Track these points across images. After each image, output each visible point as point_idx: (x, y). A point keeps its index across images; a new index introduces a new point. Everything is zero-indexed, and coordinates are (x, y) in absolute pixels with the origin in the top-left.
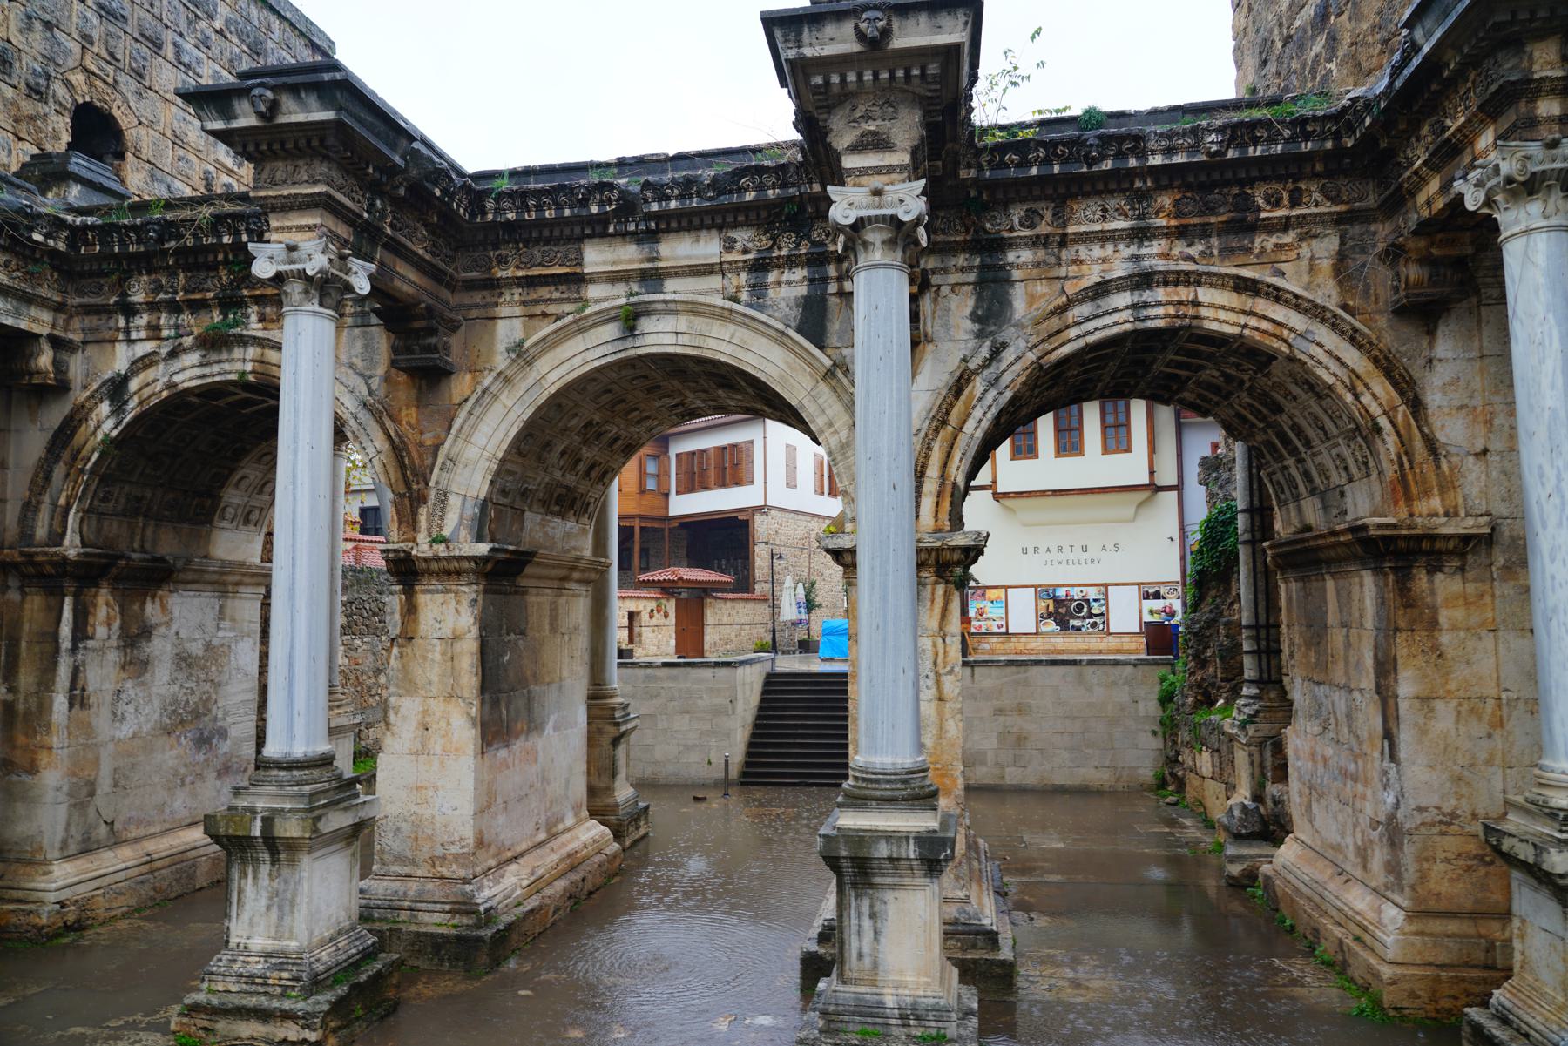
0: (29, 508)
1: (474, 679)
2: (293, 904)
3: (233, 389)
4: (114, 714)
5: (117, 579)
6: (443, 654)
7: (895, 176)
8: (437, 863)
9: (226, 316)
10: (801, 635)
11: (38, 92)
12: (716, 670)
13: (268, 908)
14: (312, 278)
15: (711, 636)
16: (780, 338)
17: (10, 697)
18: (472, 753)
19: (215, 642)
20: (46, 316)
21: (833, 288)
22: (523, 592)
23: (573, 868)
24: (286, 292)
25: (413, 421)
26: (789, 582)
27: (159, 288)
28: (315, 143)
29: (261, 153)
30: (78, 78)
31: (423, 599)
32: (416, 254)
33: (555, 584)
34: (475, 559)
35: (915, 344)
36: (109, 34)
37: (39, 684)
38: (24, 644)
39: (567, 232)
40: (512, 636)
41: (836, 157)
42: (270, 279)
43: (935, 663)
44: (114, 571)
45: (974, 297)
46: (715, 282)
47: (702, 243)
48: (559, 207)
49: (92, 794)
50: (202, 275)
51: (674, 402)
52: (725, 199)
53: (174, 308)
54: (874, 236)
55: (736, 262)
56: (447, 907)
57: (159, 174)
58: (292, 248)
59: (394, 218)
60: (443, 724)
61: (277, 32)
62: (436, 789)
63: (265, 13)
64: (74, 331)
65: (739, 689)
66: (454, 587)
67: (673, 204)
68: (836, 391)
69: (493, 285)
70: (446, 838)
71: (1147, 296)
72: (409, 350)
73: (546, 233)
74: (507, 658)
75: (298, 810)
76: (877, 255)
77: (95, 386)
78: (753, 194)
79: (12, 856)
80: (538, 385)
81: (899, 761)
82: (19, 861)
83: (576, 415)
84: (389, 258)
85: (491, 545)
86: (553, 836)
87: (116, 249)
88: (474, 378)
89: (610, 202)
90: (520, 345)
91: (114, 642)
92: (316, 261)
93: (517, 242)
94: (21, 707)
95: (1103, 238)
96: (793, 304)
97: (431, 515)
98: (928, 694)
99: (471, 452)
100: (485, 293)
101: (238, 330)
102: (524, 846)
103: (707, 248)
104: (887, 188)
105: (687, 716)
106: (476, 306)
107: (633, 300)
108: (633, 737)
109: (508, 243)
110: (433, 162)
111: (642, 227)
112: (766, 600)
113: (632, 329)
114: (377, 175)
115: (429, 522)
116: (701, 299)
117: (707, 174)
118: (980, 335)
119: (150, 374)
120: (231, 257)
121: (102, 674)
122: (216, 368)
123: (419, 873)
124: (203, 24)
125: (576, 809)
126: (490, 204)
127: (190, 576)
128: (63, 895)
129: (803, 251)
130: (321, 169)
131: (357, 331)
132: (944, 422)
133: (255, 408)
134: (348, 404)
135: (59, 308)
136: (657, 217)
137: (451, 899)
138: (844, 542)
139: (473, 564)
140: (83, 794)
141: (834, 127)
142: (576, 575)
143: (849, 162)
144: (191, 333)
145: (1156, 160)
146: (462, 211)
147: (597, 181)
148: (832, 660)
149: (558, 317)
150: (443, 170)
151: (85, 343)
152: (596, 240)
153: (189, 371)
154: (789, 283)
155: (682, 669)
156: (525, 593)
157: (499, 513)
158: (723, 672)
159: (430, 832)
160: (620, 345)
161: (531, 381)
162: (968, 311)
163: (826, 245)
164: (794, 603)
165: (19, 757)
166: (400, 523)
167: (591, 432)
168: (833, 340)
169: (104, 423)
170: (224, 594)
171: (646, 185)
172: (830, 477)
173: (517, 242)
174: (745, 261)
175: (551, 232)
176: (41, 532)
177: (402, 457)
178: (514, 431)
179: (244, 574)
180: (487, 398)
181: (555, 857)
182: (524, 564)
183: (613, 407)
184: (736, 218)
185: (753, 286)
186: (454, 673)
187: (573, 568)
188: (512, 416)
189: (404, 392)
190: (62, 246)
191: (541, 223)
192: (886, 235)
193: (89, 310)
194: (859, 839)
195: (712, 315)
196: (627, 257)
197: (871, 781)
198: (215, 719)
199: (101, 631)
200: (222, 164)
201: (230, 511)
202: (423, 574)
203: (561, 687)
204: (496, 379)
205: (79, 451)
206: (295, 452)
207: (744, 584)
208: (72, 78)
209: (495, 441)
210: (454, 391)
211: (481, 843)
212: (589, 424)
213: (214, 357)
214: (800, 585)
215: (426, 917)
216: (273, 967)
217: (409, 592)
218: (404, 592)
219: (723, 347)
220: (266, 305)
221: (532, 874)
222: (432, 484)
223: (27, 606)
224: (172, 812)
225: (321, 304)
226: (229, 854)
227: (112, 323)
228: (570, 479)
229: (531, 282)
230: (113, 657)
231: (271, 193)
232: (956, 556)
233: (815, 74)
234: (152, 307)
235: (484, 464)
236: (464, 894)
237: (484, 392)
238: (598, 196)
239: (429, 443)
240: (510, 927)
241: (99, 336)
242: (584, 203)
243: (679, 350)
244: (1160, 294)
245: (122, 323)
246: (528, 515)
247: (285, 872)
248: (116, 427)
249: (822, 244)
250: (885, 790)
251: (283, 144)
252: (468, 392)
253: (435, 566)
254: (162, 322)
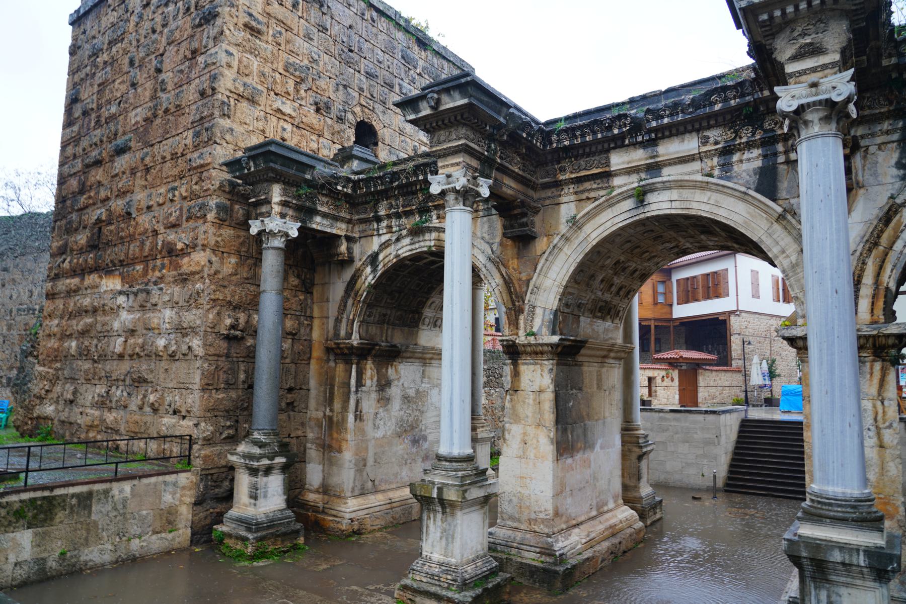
0: (338, 320)
1: (552, 416)
2: (453, 538)
3: (426, 256)
4: (375, 425)
5: (375, 356)
6: (534, 400)
7: (826, 72)
8: (532, 523)
9: (421, 218)
10: (766, 394)
11: (341, 119)
12: (706, 416)
13: (441, 538)
14: (459, 191)
15: (702, 394)
16: (743, 197)
17: (331, 414)
18: (551, 459)
19: (421, 389)
20: (344, 226)
21: (781, 159)
22: (580, 365)
23: (613, 535)
24: (446, 201)
25: (516, 267)
26: (756, 359)
27: (391, 207)
28: (459, 118)
29: (433, 128)
30: (358, 110)
31: (523, 368)
32: (514, 172)
33: (600, 360)
34: (551, 345)
35: (849, 190)
36: (371, 86)
37: (342, 408)
38: (336, 388)
39: (600, 147)
40: (574, 391)
41: (782, 66)
42: (439, 194)
43: (876, 420)
44: (374, 352)
45: (898, 151)
46: (696, 165)
47: (686, 142)
48: (594, 133)
49: (365, 465)
50: (410, 197)
51: (672, 245)
52: (701, 112)
53: (398, 216)
54: (813, 116)
55: (710, 151)
56: (538, 550)
57: (393, 150)
58: (449, 176)
59: (502, 153)
60: (534, 441)
61: (446, 69)
62: (531, 479)
63: (441, 60)
64: (355, 233)
65: (722, 428)
66: (540, 361)
67: (666, 121)
68: (786, 229)
69: (558, 185)
70: (537, 509)
72: (512, 227)
73: (587, 150)
74: (571, 404)
75: (455, 485)
76: (816, 129)
77: (364, 259)
78: (720, 105)
79: (332, 493)
80: (585, 241)
81: (849, 491)
82: (334, 495)
83: (609, 257)
84: (500, 176)
85: (560, 337)
86: (601, 514)
87: (372, 189)
88: (548, 240)
89: (625, 125)
90: (574, 218)
91: (374, 388)
92: (461, 181)
93: (571, 158)
94: (335, 419)
96: (752, 173)
97: (526, 320)
98: (870, 442)
99: (548, 283)
100: (553, 190)
101: (427, 224)
102: (583, 518)
103: (690, 145)
104: (821, 81)
105: (687, 445)
106: (549, 198)
107: (642, 183)
108: (651, 456)
109: (566, 159)
110: (521, 118)
111: (646, 138)
112: (740, 371)
113: (642, 201)
114: (492, 130)
115: (525, 324)
116: (687, 178)
117: (687, 98)
119: (388, 251)
120: (423, 186)
121: (369, 404)
122: (417, 245)
123: (522, 527)
124: (412, 72)
125: (615, 499)
126: (554, 138)
127: (408, 355)
128: (353, 515)
129: (758, 137)
130: (463, 131)
131: (485, 219)
132: (876, 244)
133: (437, 265)
134: (481, 260)
135: (349, 222)
136: (656, 130)
137: (540, 545)
138: (797, 332)
139: (550, 348)
140: (361, 465)
141: (778, 47)
142: (612, 355)
143: (790, 68)
144: (406, 228)
146: (538, 144)
147: (616, 114)
148: (789, 412)
149: (596, 199)
150: (527, 122)
151: (360, 238)
152: (617, 150)
153: (405, 248)
154: (749, 160)
155: (683, 414)
156: (581, 366)
157: (565, 318)
158: (711, 417)
159: (528, 504)
160: (635, 212)
161: (581, 238)
162: (893, 161)
163: (775, 131)
164: (760, 373)
165: (334, 444)
166: (510, 325)
167: (619, 267)
168: (783, 194)
169: (369, 277)
170: (425, 364)
171: (648, 111)
172: (783, 290)
173: (571, 158)
174: (716, 150)
175: (590, 149)
176: (343, 333)
177: (510, 287)
178: (572, 268)
179: (434, 354)
180: (556, 251)
181: (601, 527)
182: (580, 348)
183: (632, 251)
184: (708, 123)
185: (723, 165)
186: (540, 412)
187: (610, 351)
188: (571, 260)
189: (511, 252)
190: (350, 191)
191: (584, 144)
192: (822, 114)
193: (362, 221)
194: (816, 545)
195: (695, 187)
196: (638, 157)
197: (825, 504)
198: (421, 430)
199: (368, 382)
200: (422, 141)
201: (427, 320)
202: (522, 354)
203: (604, 423)
204: (560, 239)
205: (358, 292)
206: (452, 287)
207: (724, 360)
208: (355, 110)
209: (561, 276)
210: (537, 248)
211: (557, 514)
212: (618, 262)
213: (416, 239)
214: (764, 362)
215: (526, 554)
216: (443, 572)
217: (515, 364)
218: (513, 364)
219: (703, 207)
220: (440, 209)
221: (588, 536)
222: (526, 302)
223: (337, 369)
224: (401, 478)
225: (464, 205)
226: (422, 506)
227: (371, 227)
228: (607, 297)
229: (579, 180)
230: (374, 396)
231: (438, 148)
232: (891, 341)
233: (762, 14)
234: (389, 216)
235: (555, 289)
236: (547, 543)
237: (554, 247)
238: (618, 123)
239: (524, 278)
240: (574, 567)
241: (366, 234)
242: (610, 128)
243: (673, 212)
245: (376, 226)
246: (582, 318)
247: (449, 519)
248: (374, 277)
249: (772, 130)
250: (838, 512)
251: (443, 121)
252: (545, 248)
253: (529, 349)
254: (393, 224)
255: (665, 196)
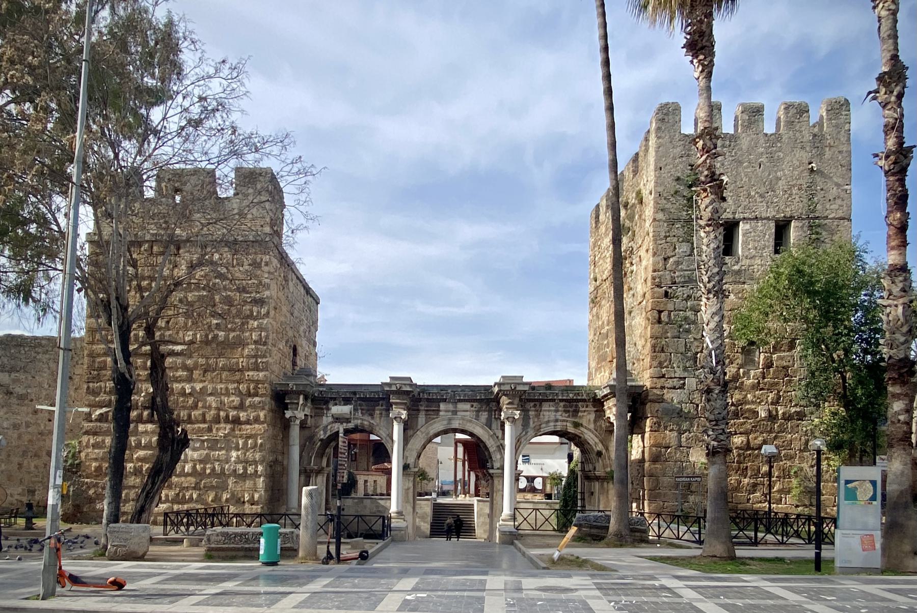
16: (482, 427)
46: (468, 413)
71: (558, 424)
95: (549, 411)
103: (467, 406)
118: (523, 430)
126: (421, 394)
145: (560, 398)
168: (493, 428)
244: (559, 423)
255: (458, 422)
